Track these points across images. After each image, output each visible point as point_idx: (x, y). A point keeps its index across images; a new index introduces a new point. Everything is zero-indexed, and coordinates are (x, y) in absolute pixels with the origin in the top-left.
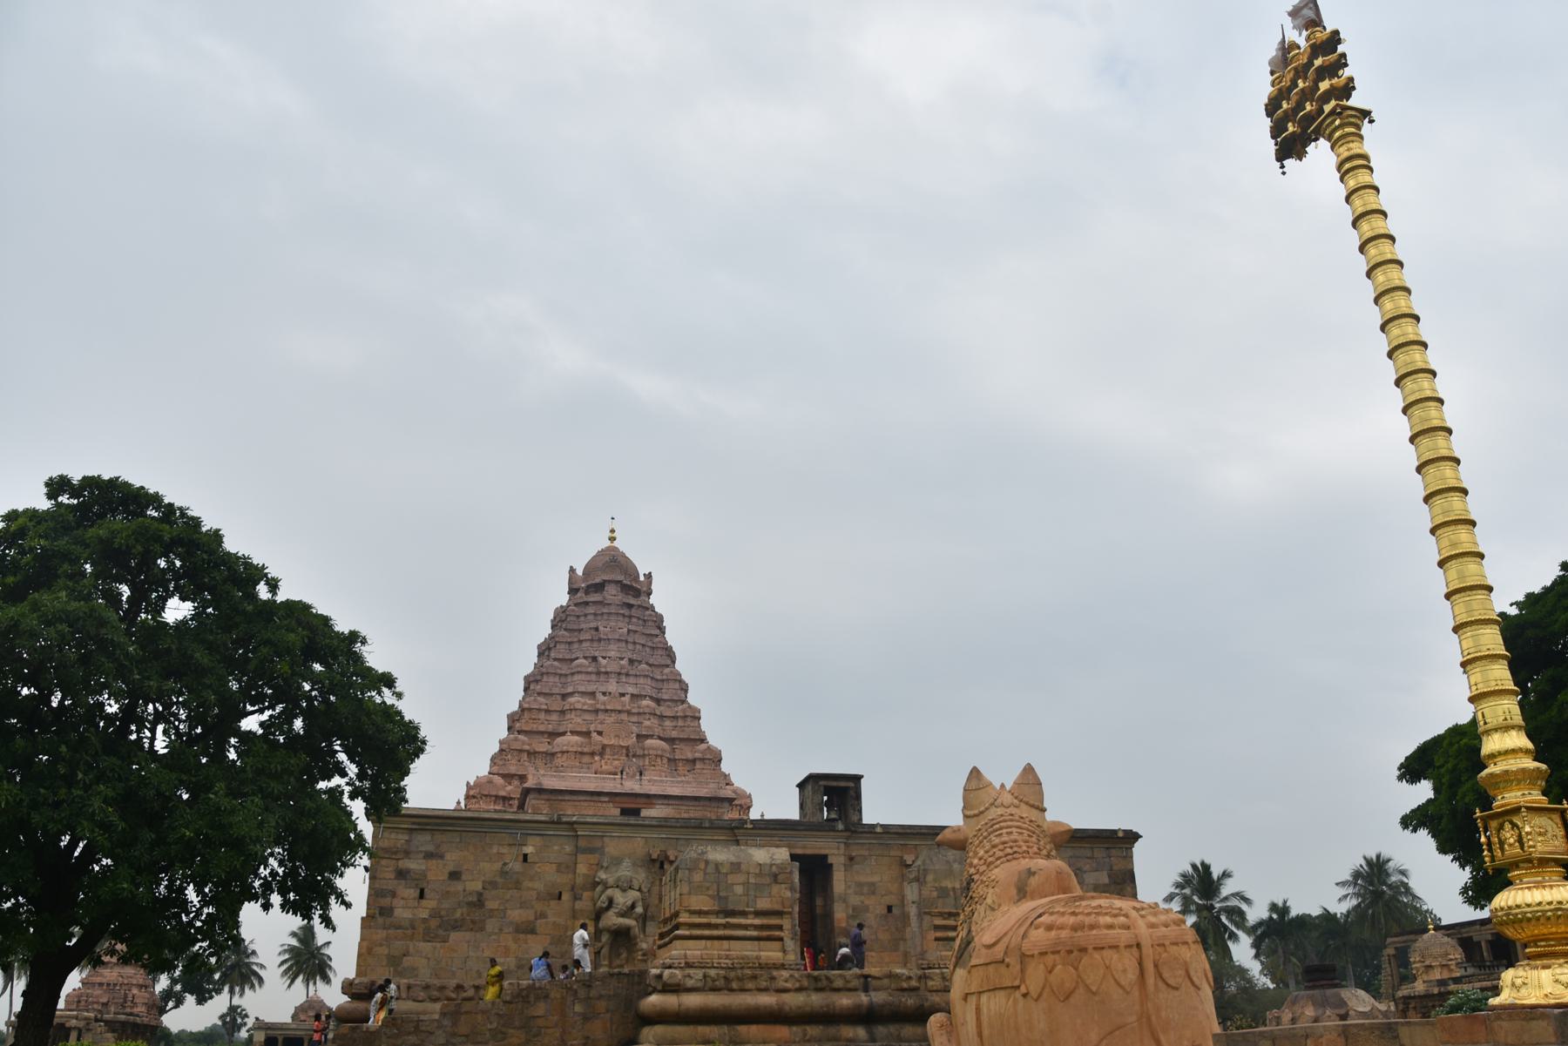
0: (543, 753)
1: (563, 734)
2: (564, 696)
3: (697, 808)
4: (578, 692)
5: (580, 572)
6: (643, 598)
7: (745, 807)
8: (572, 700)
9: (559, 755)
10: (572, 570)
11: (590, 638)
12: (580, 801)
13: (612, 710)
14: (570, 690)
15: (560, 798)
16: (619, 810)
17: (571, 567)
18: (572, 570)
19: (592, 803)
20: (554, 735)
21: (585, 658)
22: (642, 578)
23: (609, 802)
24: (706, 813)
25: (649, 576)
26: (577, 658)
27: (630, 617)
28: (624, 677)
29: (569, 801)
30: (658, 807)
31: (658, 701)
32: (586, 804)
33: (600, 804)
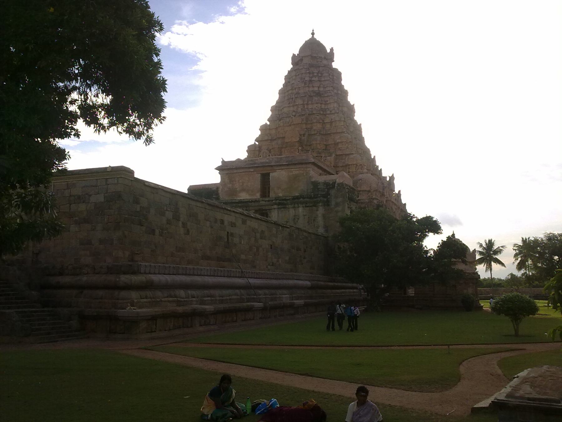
3: (296, 169)
7: (358, 165)
16: (260, 175)
22: (328, 51)
25: (332, 50)
32: (244, 174)
33: (250, 173)
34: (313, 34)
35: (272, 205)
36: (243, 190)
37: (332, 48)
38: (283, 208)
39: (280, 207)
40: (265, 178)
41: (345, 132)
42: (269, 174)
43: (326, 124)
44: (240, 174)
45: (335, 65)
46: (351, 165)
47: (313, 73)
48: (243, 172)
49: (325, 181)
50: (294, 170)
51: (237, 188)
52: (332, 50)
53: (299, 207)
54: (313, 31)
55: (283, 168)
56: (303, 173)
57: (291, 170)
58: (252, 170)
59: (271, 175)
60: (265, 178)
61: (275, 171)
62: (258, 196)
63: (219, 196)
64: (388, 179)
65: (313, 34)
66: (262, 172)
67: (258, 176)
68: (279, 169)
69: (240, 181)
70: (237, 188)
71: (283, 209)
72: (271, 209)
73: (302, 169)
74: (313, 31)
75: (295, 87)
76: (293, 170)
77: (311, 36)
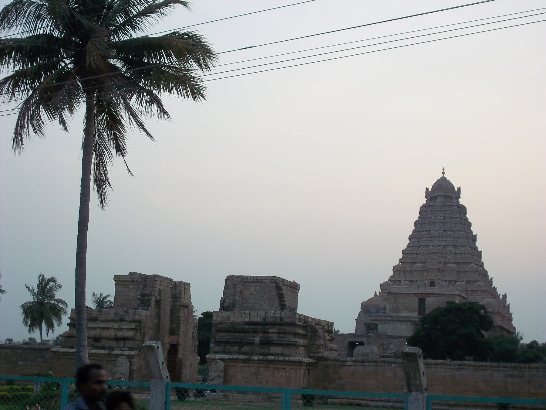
0: (409, 271)
1: (416, 263)
2: (419, 247)
4: (423, 246)
5: (430, 190)
6: (455, 201)
8: (420, 249)
9: (414, 272)
10: (427, 189)
11: (428, 222)
14: (420, 245)
17: (427, 188)
18: (427, 189)
20: (414, 263)
21: (426, 231)
22: (456, 190)
25: (459, 189)
26: (423, 231)
27: (446, 211)
28: (441, 238)
30: (431, 297)
31: (455, 247)
34: (443, 173)
37: (460, 187)
40: (422, 301)
41: (472, 262)
42: (424, 299)
43: (457, 254)
45: (462, 201)
46: (478, 290)
47: (446, 211)
52: (459, 189)
54: (443, 170)
59: (427, 300)
60: (422, 301)
64: (501, 297)
65: (443, 173)
66: (419, 298)
67: (417, 300)
69: (403, 302)
74: (443, 170)
75: (433, 221)
77: (441, 175)
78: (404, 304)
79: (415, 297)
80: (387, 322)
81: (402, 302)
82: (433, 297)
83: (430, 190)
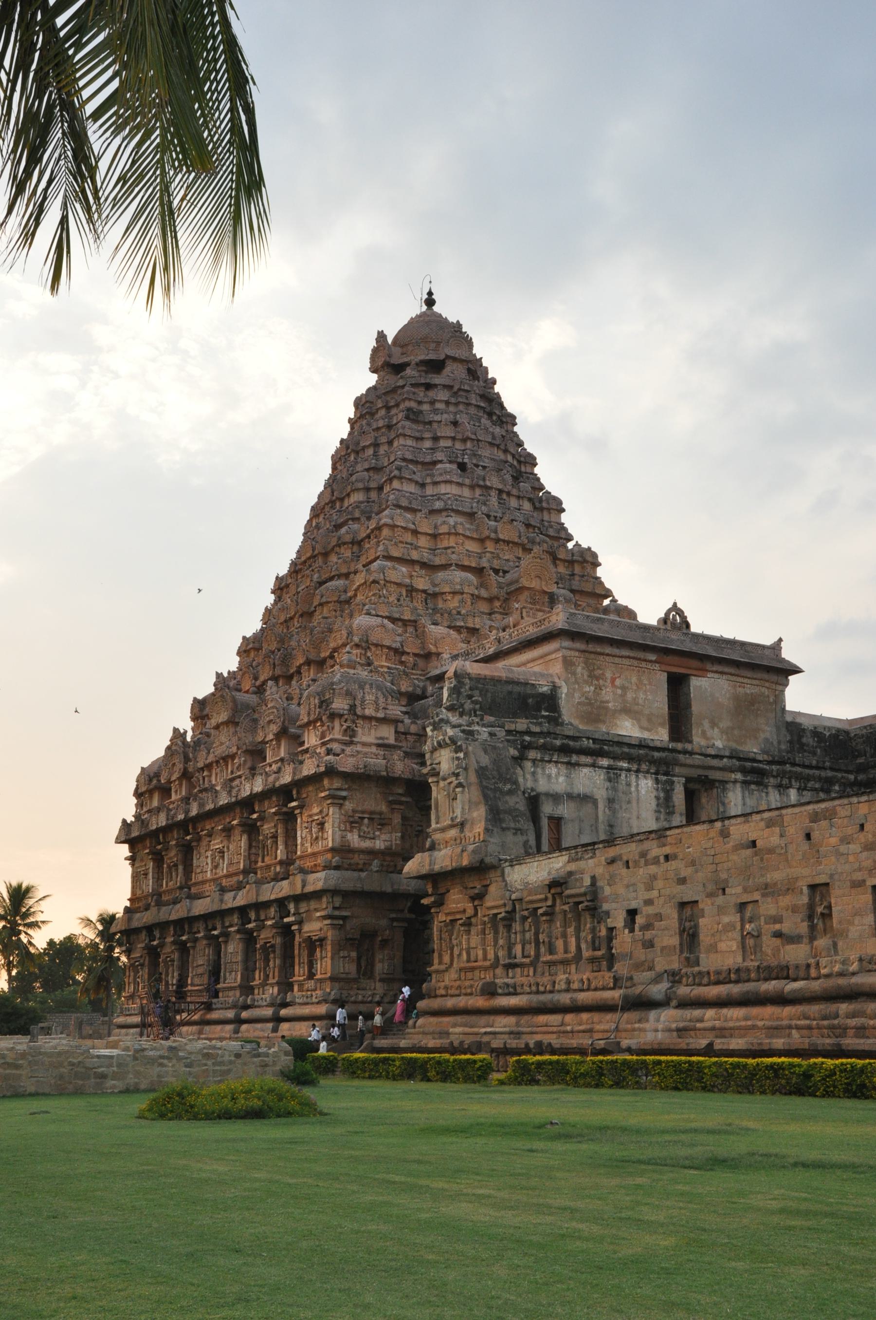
3: (754, 682)
5: (390, 340)
10: (381, 336)
12: (622, 657)
13: (504, 541)
15: (599, 650)
16: (666, 674)
18: (381, 336)
19: (635, 663)
23: (656, 662)
24: (763, 690)
29: (608, 655)
30: (710, 675)
33: (644, 664)
34: (430, 302)
35: (732, 772)
36: (627, 711)
38: (754, 783)
39: (749, 778)
44: (617, 660)
48: (629, 657)
49: (815, 728)
50: (749, 681)
51: (608, 702)
53: (791, 787)
55: (726, 670)
56: (768, 696)
57: (741, 680)
58: (653, 657)
59: (696, 683)
61: (702, 672)
62: (661, 735)
63: (560, 716)
65: (430, 302)
68: (716, 672)
69: (618, 682)
70: (608, 702)
71: (753, 787)
72: (726, 782)
73: (767, 684)
76: (746, 681)
77: (417, 308)
78: (619, 691)
79: (657, 667)
80: (589, 760)
81: (613, 680)
82: (716, 676)
83: (390, 340)
